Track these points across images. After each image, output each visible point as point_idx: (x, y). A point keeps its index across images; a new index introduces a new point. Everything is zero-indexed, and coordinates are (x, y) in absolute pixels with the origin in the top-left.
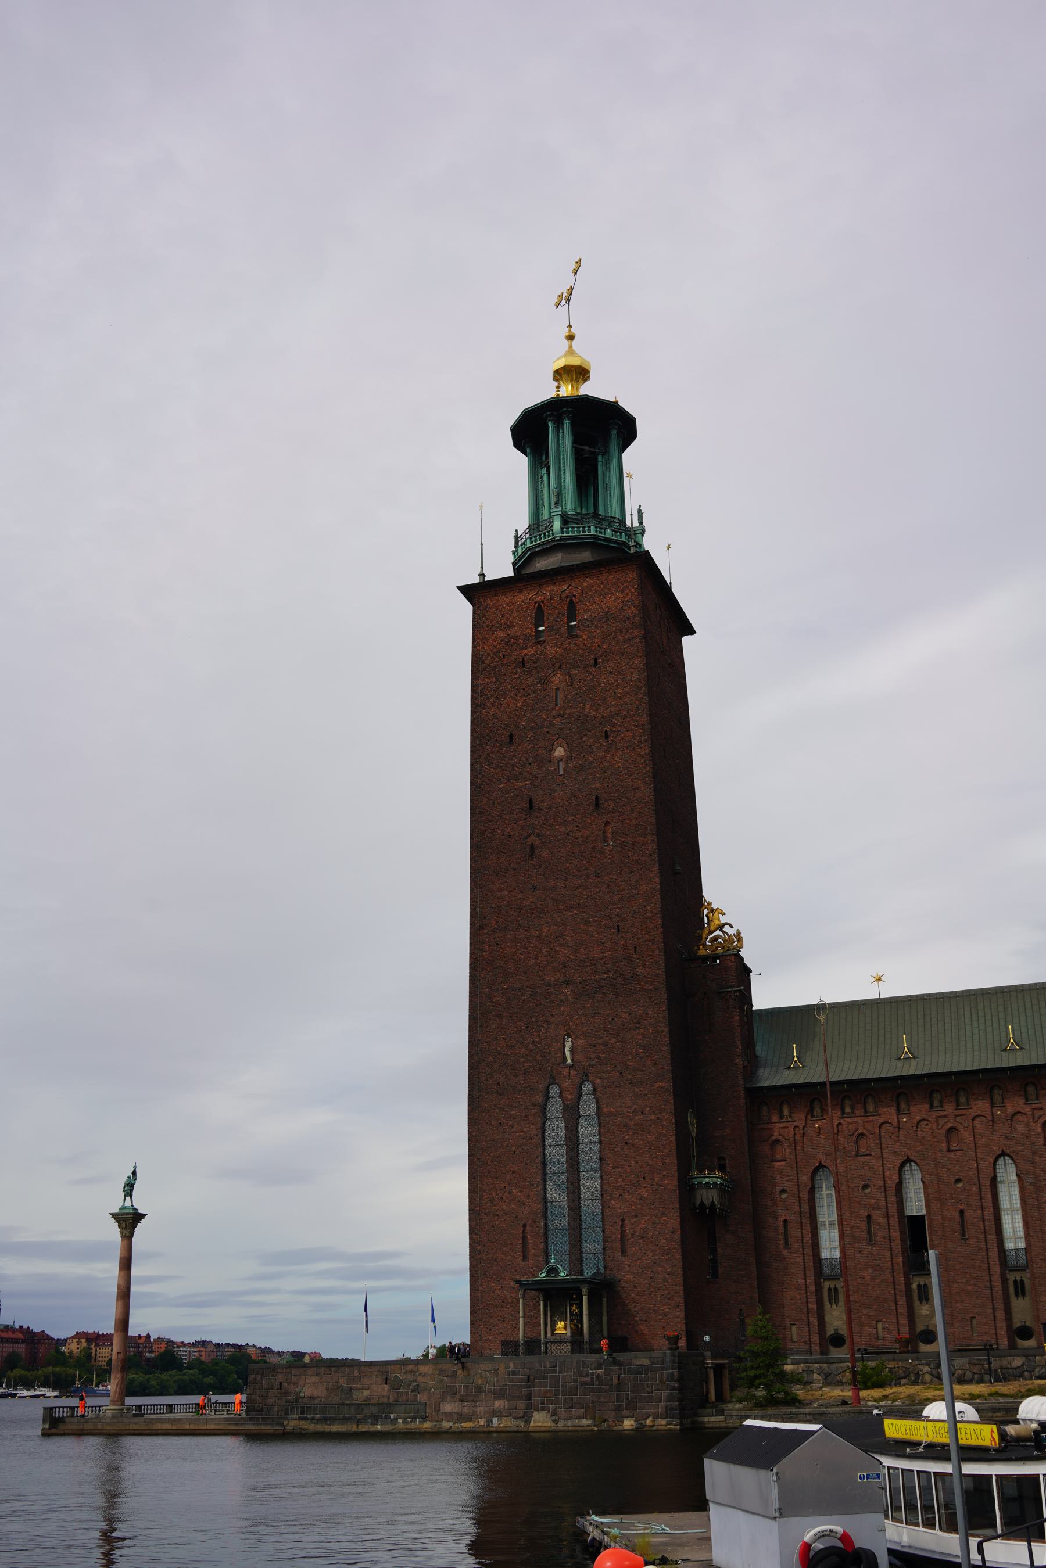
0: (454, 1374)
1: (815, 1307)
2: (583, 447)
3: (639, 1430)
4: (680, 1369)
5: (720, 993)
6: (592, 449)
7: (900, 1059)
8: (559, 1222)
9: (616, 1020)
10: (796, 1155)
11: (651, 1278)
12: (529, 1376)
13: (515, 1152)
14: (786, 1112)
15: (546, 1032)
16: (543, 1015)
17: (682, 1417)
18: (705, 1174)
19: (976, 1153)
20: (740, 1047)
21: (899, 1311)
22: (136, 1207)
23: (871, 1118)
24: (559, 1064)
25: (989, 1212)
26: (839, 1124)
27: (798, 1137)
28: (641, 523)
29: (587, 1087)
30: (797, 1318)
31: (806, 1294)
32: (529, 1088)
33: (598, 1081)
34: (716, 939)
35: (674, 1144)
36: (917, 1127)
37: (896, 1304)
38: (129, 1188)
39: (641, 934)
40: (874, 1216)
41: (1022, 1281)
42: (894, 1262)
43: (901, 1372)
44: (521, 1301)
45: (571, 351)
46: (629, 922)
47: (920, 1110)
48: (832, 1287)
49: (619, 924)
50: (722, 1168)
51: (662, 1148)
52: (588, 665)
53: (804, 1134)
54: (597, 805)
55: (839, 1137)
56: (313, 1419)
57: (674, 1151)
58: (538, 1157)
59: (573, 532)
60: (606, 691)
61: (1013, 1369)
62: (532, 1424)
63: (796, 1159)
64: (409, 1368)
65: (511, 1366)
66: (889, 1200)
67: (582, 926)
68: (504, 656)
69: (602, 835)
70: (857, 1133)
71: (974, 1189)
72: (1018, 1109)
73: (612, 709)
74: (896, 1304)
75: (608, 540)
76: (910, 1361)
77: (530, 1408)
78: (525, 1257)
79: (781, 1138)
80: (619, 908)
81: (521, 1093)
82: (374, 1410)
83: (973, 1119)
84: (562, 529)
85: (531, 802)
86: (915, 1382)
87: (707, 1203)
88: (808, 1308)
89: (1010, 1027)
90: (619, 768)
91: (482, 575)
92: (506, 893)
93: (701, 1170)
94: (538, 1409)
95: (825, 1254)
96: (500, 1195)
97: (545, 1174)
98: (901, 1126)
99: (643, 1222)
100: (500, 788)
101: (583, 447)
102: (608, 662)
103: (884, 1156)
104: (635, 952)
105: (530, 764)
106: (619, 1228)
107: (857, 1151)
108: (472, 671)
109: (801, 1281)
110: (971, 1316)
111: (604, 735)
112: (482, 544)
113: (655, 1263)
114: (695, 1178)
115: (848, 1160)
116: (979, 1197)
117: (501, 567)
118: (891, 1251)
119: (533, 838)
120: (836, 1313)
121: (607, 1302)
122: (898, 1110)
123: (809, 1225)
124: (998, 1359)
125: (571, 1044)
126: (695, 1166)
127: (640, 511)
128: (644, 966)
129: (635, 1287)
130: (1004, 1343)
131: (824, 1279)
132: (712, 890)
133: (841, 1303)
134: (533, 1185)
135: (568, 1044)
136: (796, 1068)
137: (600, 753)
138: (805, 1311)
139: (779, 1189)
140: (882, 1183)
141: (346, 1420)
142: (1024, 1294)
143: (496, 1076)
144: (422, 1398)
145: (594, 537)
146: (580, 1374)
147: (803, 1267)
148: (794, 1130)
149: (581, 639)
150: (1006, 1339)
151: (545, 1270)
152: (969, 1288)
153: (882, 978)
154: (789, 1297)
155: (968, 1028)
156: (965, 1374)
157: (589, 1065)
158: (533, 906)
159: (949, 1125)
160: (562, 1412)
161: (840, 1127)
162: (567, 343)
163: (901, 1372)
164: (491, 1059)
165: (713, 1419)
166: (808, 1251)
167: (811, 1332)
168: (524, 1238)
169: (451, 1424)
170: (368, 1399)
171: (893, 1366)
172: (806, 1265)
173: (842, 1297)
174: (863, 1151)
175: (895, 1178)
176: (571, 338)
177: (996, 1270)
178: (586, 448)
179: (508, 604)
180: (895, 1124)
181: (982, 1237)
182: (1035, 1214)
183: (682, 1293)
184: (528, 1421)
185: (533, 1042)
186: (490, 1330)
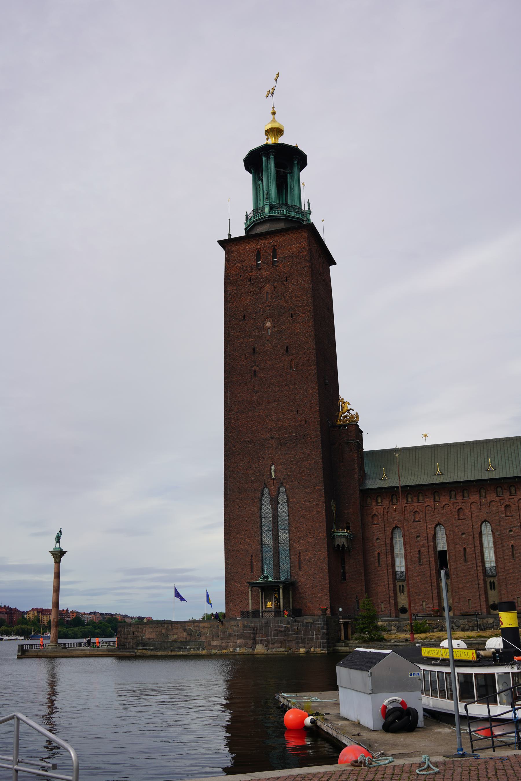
0: (218, 627)
1: (393, 595)
2: (280, 170)
3: (307, 653)
4: (327, 624)
5: (347, 443)
6: (285, 171)
7: (435, 475)
8: (268, 554)
9: (296, 456)
10: (384, 522)
11: (313, 581)
12: (254, 628)
13: (247, 521)
14: (379, 501)
15: (262, 462)
16: (261, 454)
17: (328, 647)
18: (340, 531)
19: (472, 520)
20: (357, 469)
21: (433, 596)
22: (62, 548)
23: (421, 504)
24: (268, 478)
25: (478, 549)
27: (385, 513)
28: (309, 208)
29: (282, 489)
30: (384, 600)
31: (389, 587)
32: (254, 490)
33: (287, 486)
34: (346, 416)
35: (324, 517)
36: (443, 508)
37: (432, 593)
38: (58, 539)
39: (309, 414)
40: (422, 551)
41: (494, 582)
42: (431, 573)
43: (434, 625)
44: (250, 592)
45: (274, 120)
47: (445, 499)
48: (401, 585)
49: (298, 409)
50: (348, 528)
51: (319, 518)
52: (283, 281)
53: (388, 511)
54: (287, 351)
55: (405, 513)
56: (149, 649)
57: (325, 520)
58: (258, 523)
59: (275, 213)
60: (292, 294)
61: (488, 624)
62: (256, 651)
63: (384, 523)
64: (196, 624)
65: (246, 623)
66: (429, 543)
67: (280, 411)
68: (241, 276)
69: (289, 366)
70: (414, 511)
72: (493, 499)
73: (295, 303)
74: (432, 593)
75: (293, 217)
76: (439, 620)
77: (255, 643)
78: (252, 571)
79: (377, 513)
80: (298, 402)
81: (250, 492)
82: (179, 644)
83: (471, 504)
84: (269, 211)
85: (254, 349)
86: (441, 631)
87: (341, 545)
88: (389, 595)
89: (490, 459)
90: (298, 332)
91: (229, 235)
92: (242, 394)
93: (338, 529)
94: (258, 644)
95: (398, 569)
97: (262, 531)
98: (435, 507)
99: (309, 554)
100: (239, 342)
101: (280, 170)
102: (292, 279)
104: (306, 423)
105: (254, 330)
106: (298, 557)
108: (225, 284)
109: (386, 582)
110: (469, 599)
111: (290, 316)
112: (229, 219)
113: (315, 574)
114: (335, 533)
115: (410, 524)
116: (473, 542)
117: (239, 231)
118: (430, 567)
119: (255, 367)
120: (403, 597)
121: (292, 593)
122: (434, 500)
123: (390, 555)
124: (481, 619)
125: (274, 468)
126: (335, 527)
127: (308, 202)
128: (310, 430)
129: (306, 585)
130: (485, 612)
131: (397, 581)
132: (343, 393)
133: (406, 593)
134: (256, 536)
135: (273, 468)
136: (385, 479)
137: (288, 325)
138: (388, 596)
139: (376, 538)
140: (426, 535)
141: (165, 649)
142: (494, 588)
144: (203, 638)
145: (286, 216)
146: (279, 627)
147: (387, 575)
148: (383, 509)
149: (279, 268)
150: (485, 610)
151: (262, 577)
152: (468, 585)
153: (427, 435)
154: (380, 590)
155: (469, 459)
156: (465, 626)
157: (283, 478)
158: (256, 401)
159: (459, 507)
160: (270, 645)
161: (406, 508)
162: (272, 116)
163: (434, 625)
165: (343, 648)
166: (390, 568)
167: (391, 606)
168: (252, 562)
169: (216, 651)
170: (176, 639)
171: (430, 623)
172: (389, 574)
173: (406, 590)
174: (417, 519)
175: (433, 533)
176: (274, 113)
177: (481, 577)
178: (282, 170)
179: (242, 250)
180: (433, 507)
181: (474, 561)
182: (500, 550)
183: (328, 588)
184: (254, 649)
185: (256, 467)
186: (235, 606)
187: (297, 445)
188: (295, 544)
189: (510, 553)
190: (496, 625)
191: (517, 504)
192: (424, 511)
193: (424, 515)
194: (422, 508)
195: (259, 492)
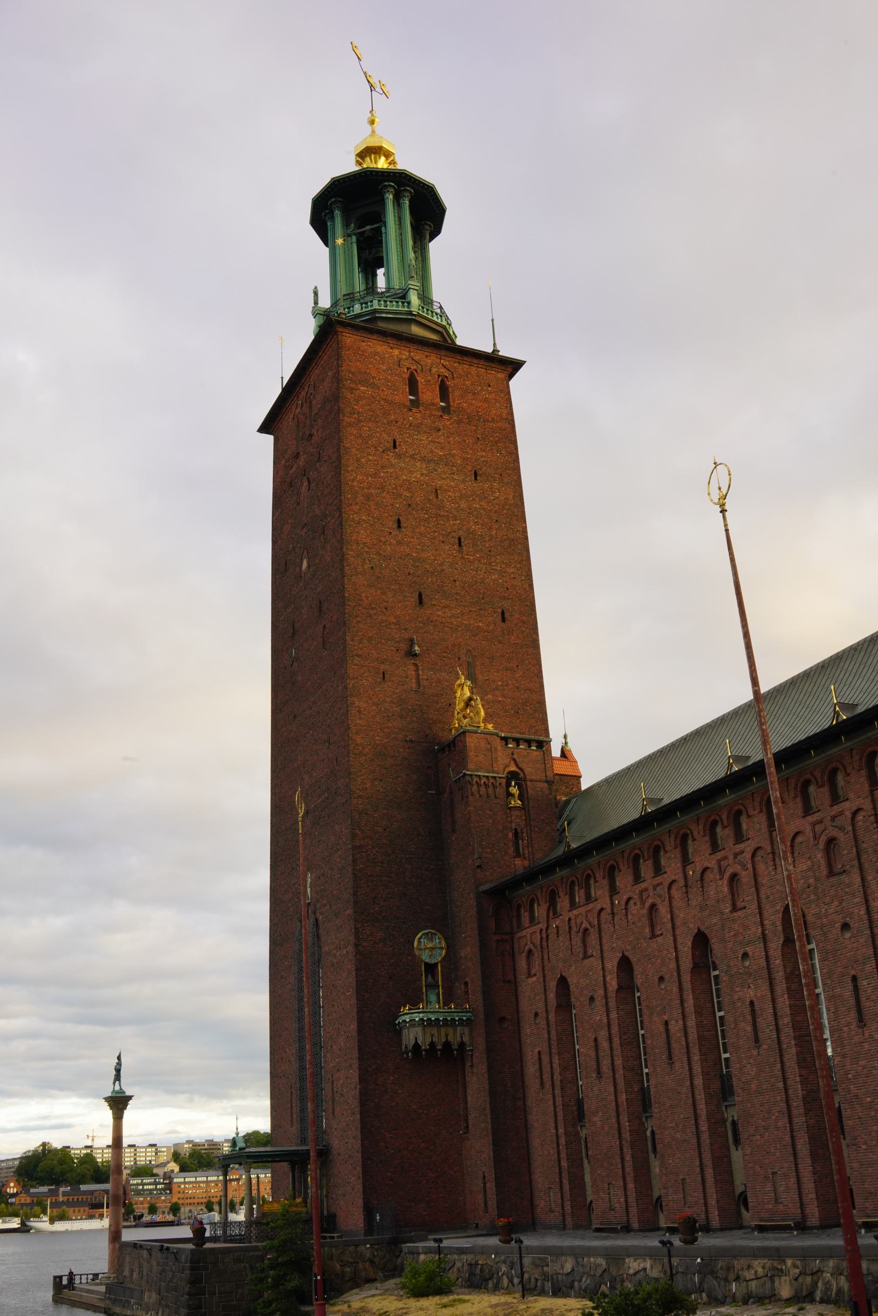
2: (364, 229)
18: (450, 1008)
19: (674, 936)
23: (591, 906)
26: (570, 919)
36: (626, 909)
40: (600, 1039)
71: (675, 989)
76: (493, 1256)
79: (532, 948)
83: (669, 888)
98: (615, 911)
101: (364, 229)
103: (605, 955)
107: (585, 952)
110: (682, 1177)
135: (309, 880)
138: (557, 1171)
147: (553, 1113)
150: (717, 1213)
152: (678, 1135)
159: (650, 901)
162: (369, 128)
172: (558, 1110)
176: (372, 122)
178: (368, 227)
180: (609, 910)
181: (685, 1059)
189: (749, 1028)
190: (577, 1281)
191: (751, 869)
192: (596, 926)
193: (597, 935)
194: (594, 918)
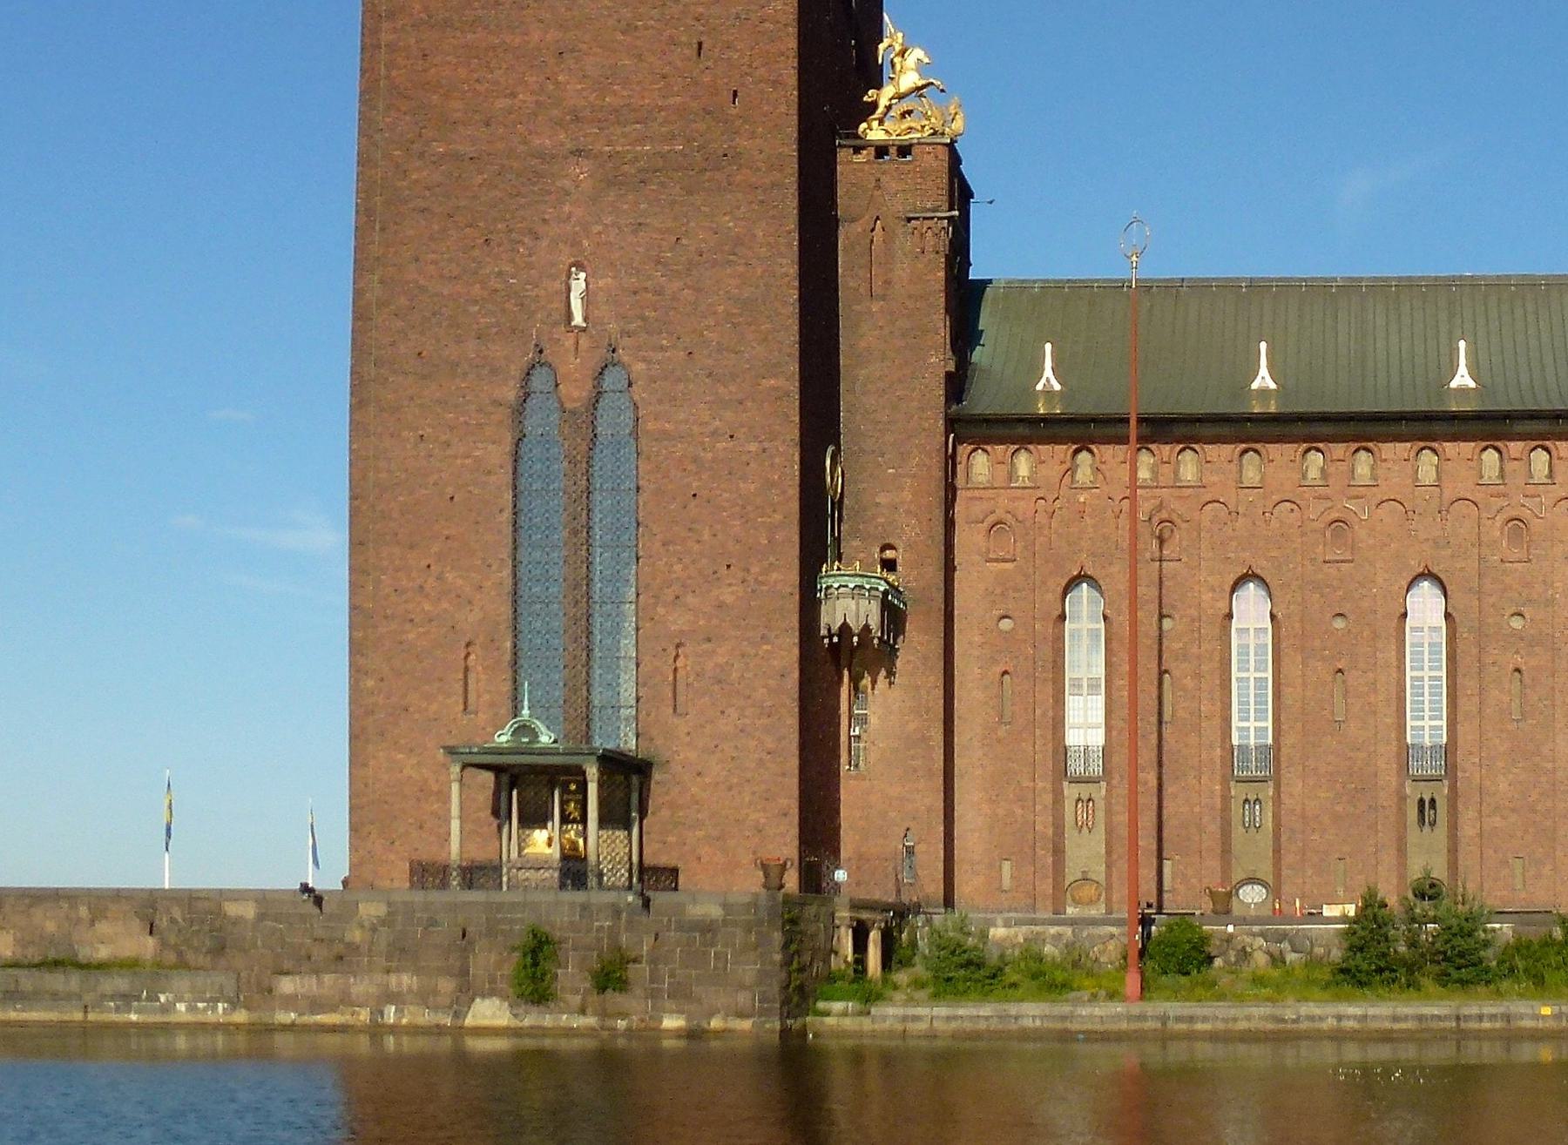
9: (684, 241)
13: (452, 498)
15: (530, 255)
24: (555, 324)
33: (640, 367)
46: (725, 38)
51: (769, 511)
58: (501, 511)
94: (483, 996)
96: (419, 582)
113: (742, 731)
125: (584, 285)
134: (489, 566)
135: (578, 285)
143: (413, 337)
164: (403, 301)
185: (500, 274)
187: (690, 193)
188: (661, 610)
195: (512, 383)
